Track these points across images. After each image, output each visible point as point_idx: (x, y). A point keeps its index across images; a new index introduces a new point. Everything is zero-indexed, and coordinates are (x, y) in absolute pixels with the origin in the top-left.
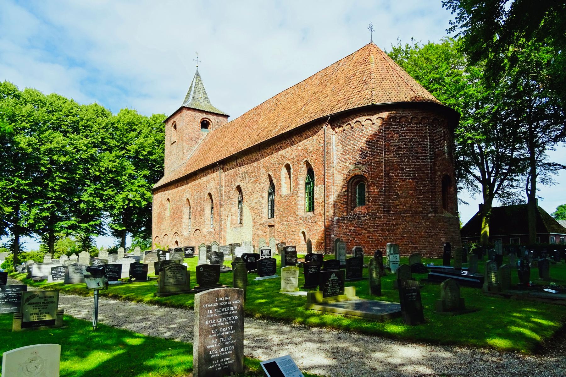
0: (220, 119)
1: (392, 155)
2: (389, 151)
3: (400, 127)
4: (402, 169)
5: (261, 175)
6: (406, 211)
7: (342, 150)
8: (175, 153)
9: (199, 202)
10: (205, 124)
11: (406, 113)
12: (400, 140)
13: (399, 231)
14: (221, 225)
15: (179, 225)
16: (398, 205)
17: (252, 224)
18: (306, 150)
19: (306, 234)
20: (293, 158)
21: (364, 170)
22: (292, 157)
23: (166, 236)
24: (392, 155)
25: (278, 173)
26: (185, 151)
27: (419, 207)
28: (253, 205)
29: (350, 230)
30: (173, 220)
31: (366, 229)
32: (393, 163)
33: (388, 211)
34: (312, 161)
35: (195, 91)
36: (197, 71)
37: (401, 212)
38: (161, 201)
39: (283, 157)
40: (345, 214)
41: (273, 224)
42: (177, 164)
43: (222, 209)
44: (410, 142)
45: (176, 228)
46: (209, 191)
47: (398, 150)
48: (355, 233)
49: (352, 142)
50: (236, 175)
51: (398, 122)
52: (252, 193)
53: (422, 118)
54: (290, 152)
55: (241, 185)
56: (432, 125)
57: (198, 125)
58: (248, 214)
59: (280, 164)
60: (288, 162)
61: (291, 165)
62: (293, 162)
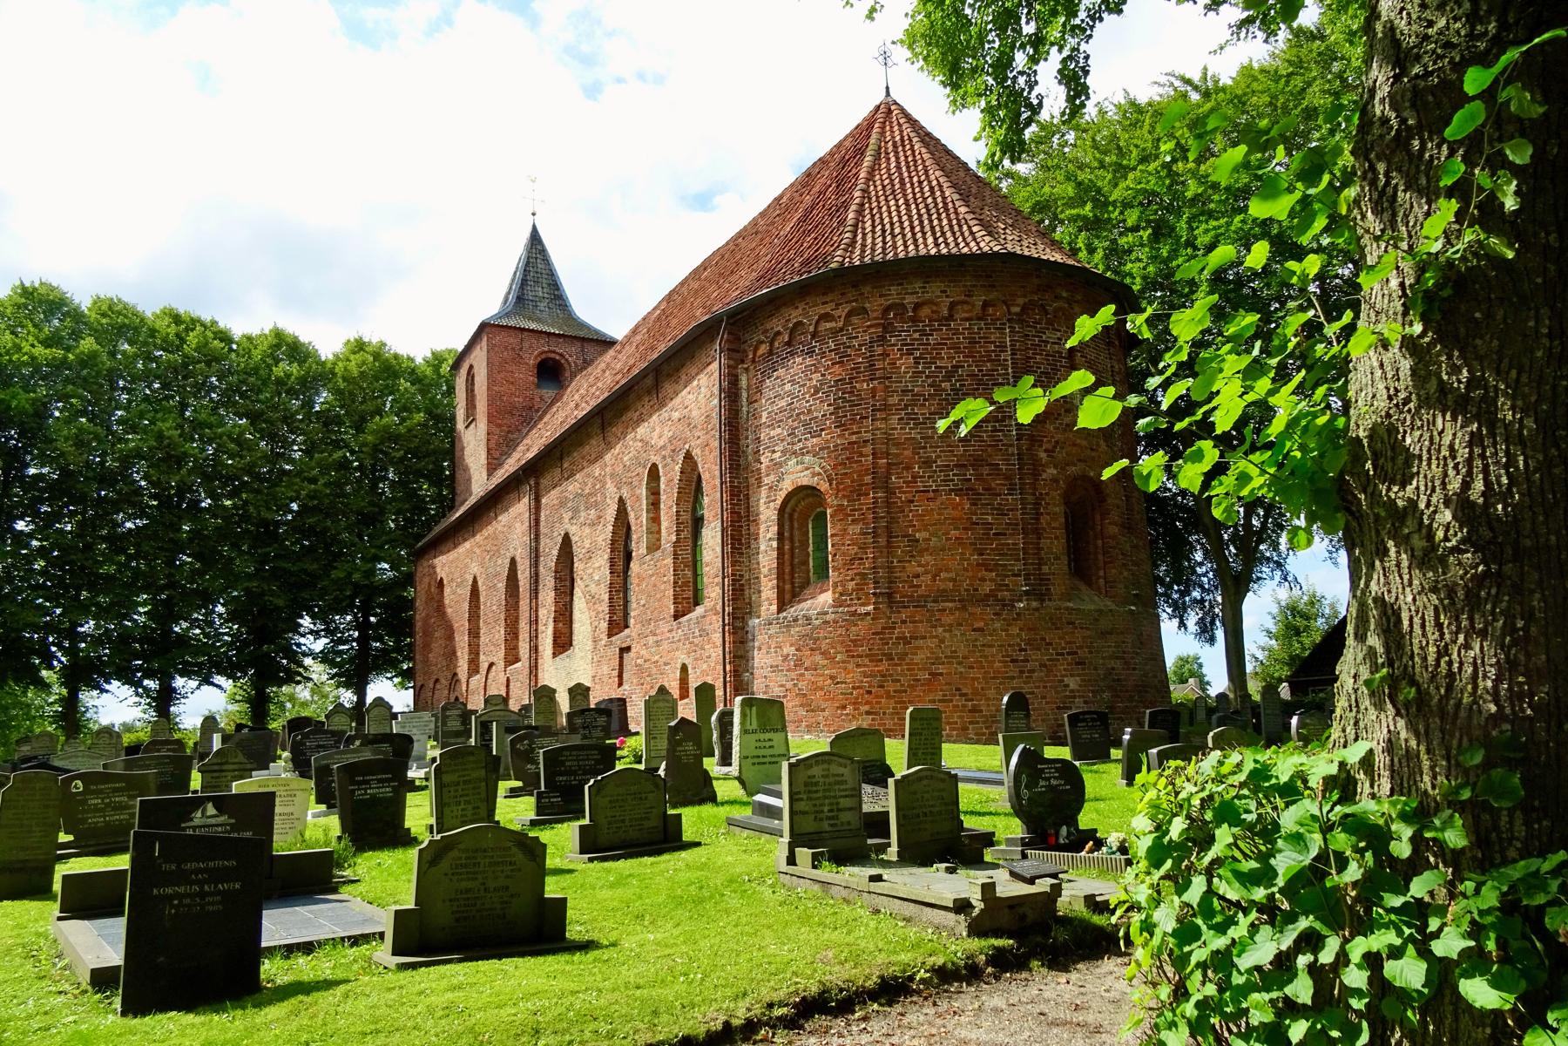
1: (894, 420)
2: (886, 407)
3: (916, 335)
4: (927, 463)
6: (943, 595)
11: (934, 290)
12: (917, 374)
13: (919, 658)
16: (917, 576)
21: (817, 469)
24: (894, 420)
27: (983, 580)
32: (898, 444)
33: (890, 595)
36: (534, 227)
40: (774, 608)
44: (948, 377)
47: (913, 403)
48: (799, 663)
49: (788, 387)
53: (986, 305)
55: (573, 530)
56: (1021, 321)
57: (525, 375)
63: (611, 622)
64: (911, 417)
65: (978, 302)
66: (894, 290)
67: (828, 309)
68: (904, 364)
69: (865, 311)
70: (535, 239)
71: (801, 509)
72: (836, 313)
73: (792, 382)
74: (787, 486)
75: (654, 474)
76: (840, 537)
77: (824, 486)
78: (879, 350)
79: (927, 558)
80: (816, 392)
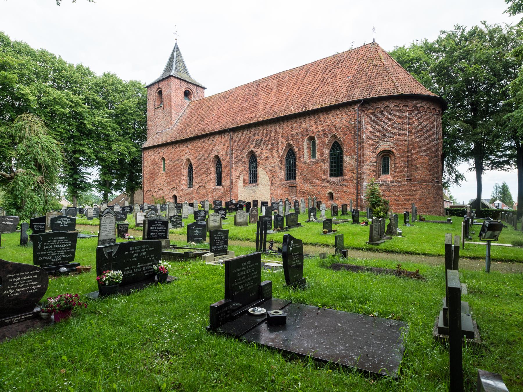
1: (413, 136)
4: (420, 148)
5: (280, 143)
6: (422, 181)
7: (371, 129)
8: (161, 116)
9: (203, 163)
10: (187, 94)
11: (424, 104)
12: (419, 125)
13: (417, 195)
14: (231, 183)
15: (177, 182)
17: (269, 184)
18: (334, 126)
19: (334, 194)
20: (319, 132)
21: (392, 146)
22: (317, 130)
23: (160, 191)
24: (413, 136)
25: (300, 143)
26: (173, 116)
28: (270, 168)
30: (169, 176)
31: (393, 193)
34: (341, 135)
35: (176, 62)
36: (176, 44)
37: (418, 181)
38: (154, 159)
39: (306, 130)
41: (295, 185)
42: (164, 127)
43: (233, 170)
44: (425, 126)
45: (173, 184)
46: (216, 154)
47: (418, 132)
50: (249, 141)
51: (418, 110)
52: (268, 158)
54: (314, 127)
55: (255, 150)
58: (264, 176)
59: (302, 135)
60: (312, 135)
61: (316, 137)
62: (319, 135)
64: (417, 136)
65: (432, 108)
66: (415, 102)
67: (397, 104)
68: (416, 122)
69: (407, 106)
70: (176, 48)
71: (385, 156)
72: (400, 105)
73: (384, 122)
74: (381, 149)
76: (397, 163)
77: (394, 151)
79: (419, 172)
80: (392, 125)
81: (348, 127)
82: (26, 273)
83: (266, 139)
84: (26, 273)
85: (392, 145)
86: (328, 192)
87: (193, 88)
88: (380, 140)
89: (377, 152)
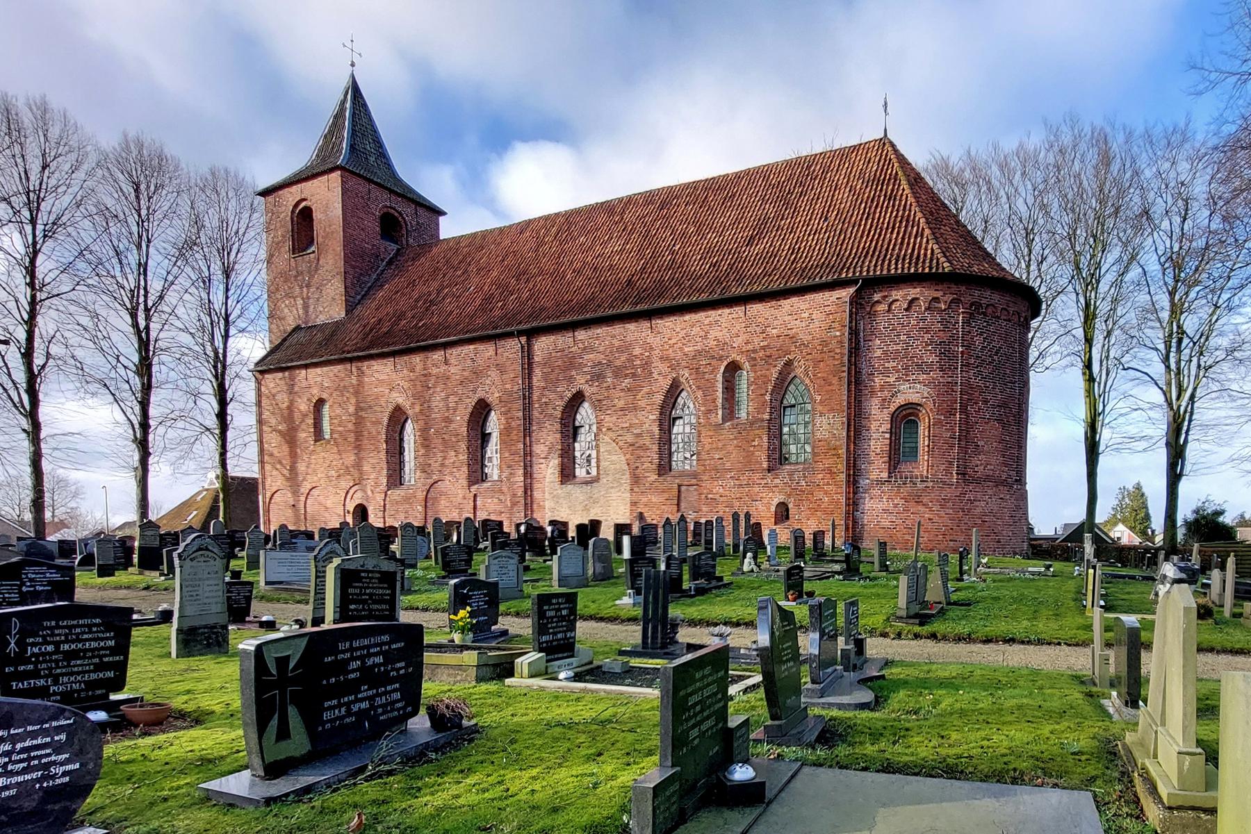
0: (421, 211)
2: (968, 365)
4: (986, 402)
5: (655, 375)
19: (790, 506)
20: (754, 351)
21: (926, 395)
22: (750, 347)
29: (896, 506)
40: (885, 475)
44: (996, 353)
46: (480, 394)
63: (660, 465)
74: (900, 400)
75: (733, 368)
78: (967, 329)
81: (824, 343)
82: (30, 728)
83: (618, 363)
84: (30, 728)
85: (926, 391)
86: (776, 502)
87: (407, 211)
88: (898, 379)
89: (892, 409)
